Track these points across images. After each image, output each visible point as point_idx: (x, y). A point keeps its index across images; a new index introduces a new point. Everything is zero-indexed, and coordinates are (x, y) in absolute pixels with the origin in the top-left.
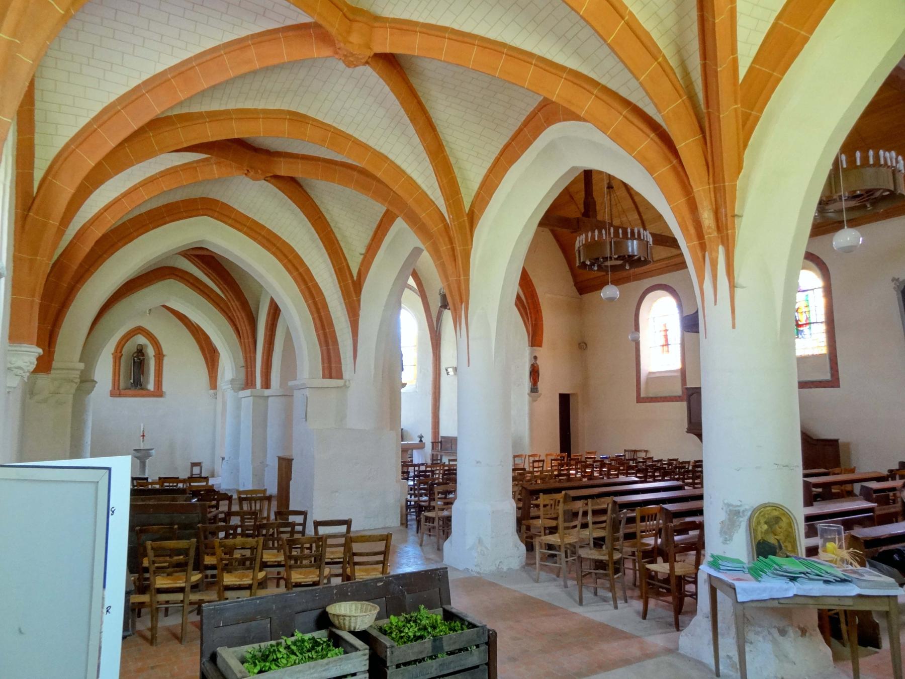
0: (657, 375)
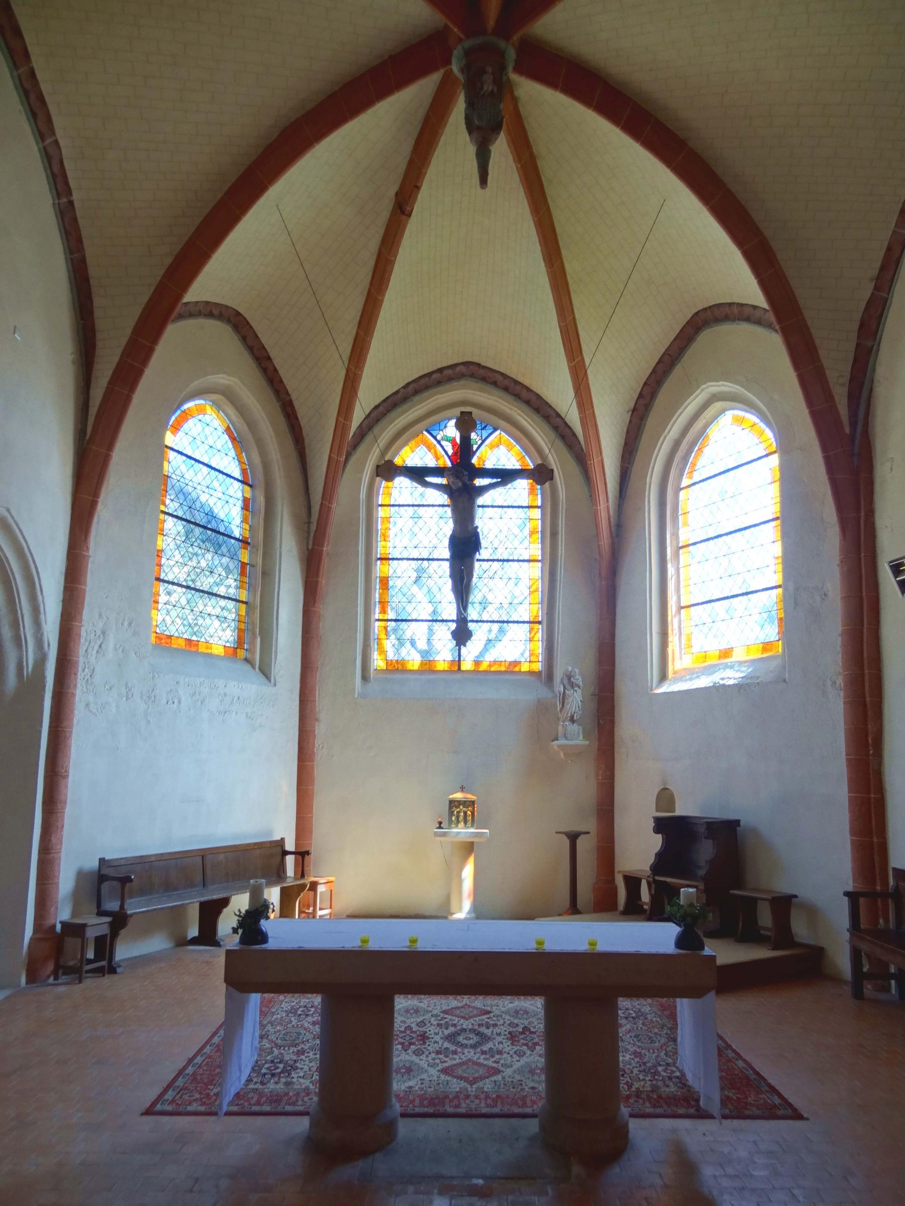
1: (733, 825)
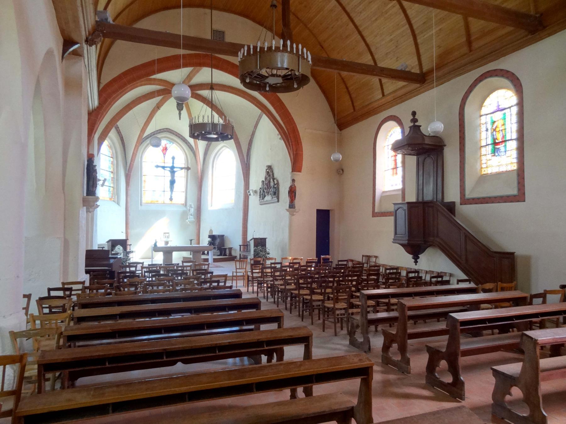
0: (388, 194)
1: (223, 236)
